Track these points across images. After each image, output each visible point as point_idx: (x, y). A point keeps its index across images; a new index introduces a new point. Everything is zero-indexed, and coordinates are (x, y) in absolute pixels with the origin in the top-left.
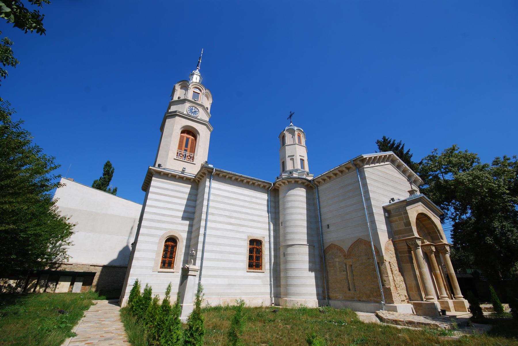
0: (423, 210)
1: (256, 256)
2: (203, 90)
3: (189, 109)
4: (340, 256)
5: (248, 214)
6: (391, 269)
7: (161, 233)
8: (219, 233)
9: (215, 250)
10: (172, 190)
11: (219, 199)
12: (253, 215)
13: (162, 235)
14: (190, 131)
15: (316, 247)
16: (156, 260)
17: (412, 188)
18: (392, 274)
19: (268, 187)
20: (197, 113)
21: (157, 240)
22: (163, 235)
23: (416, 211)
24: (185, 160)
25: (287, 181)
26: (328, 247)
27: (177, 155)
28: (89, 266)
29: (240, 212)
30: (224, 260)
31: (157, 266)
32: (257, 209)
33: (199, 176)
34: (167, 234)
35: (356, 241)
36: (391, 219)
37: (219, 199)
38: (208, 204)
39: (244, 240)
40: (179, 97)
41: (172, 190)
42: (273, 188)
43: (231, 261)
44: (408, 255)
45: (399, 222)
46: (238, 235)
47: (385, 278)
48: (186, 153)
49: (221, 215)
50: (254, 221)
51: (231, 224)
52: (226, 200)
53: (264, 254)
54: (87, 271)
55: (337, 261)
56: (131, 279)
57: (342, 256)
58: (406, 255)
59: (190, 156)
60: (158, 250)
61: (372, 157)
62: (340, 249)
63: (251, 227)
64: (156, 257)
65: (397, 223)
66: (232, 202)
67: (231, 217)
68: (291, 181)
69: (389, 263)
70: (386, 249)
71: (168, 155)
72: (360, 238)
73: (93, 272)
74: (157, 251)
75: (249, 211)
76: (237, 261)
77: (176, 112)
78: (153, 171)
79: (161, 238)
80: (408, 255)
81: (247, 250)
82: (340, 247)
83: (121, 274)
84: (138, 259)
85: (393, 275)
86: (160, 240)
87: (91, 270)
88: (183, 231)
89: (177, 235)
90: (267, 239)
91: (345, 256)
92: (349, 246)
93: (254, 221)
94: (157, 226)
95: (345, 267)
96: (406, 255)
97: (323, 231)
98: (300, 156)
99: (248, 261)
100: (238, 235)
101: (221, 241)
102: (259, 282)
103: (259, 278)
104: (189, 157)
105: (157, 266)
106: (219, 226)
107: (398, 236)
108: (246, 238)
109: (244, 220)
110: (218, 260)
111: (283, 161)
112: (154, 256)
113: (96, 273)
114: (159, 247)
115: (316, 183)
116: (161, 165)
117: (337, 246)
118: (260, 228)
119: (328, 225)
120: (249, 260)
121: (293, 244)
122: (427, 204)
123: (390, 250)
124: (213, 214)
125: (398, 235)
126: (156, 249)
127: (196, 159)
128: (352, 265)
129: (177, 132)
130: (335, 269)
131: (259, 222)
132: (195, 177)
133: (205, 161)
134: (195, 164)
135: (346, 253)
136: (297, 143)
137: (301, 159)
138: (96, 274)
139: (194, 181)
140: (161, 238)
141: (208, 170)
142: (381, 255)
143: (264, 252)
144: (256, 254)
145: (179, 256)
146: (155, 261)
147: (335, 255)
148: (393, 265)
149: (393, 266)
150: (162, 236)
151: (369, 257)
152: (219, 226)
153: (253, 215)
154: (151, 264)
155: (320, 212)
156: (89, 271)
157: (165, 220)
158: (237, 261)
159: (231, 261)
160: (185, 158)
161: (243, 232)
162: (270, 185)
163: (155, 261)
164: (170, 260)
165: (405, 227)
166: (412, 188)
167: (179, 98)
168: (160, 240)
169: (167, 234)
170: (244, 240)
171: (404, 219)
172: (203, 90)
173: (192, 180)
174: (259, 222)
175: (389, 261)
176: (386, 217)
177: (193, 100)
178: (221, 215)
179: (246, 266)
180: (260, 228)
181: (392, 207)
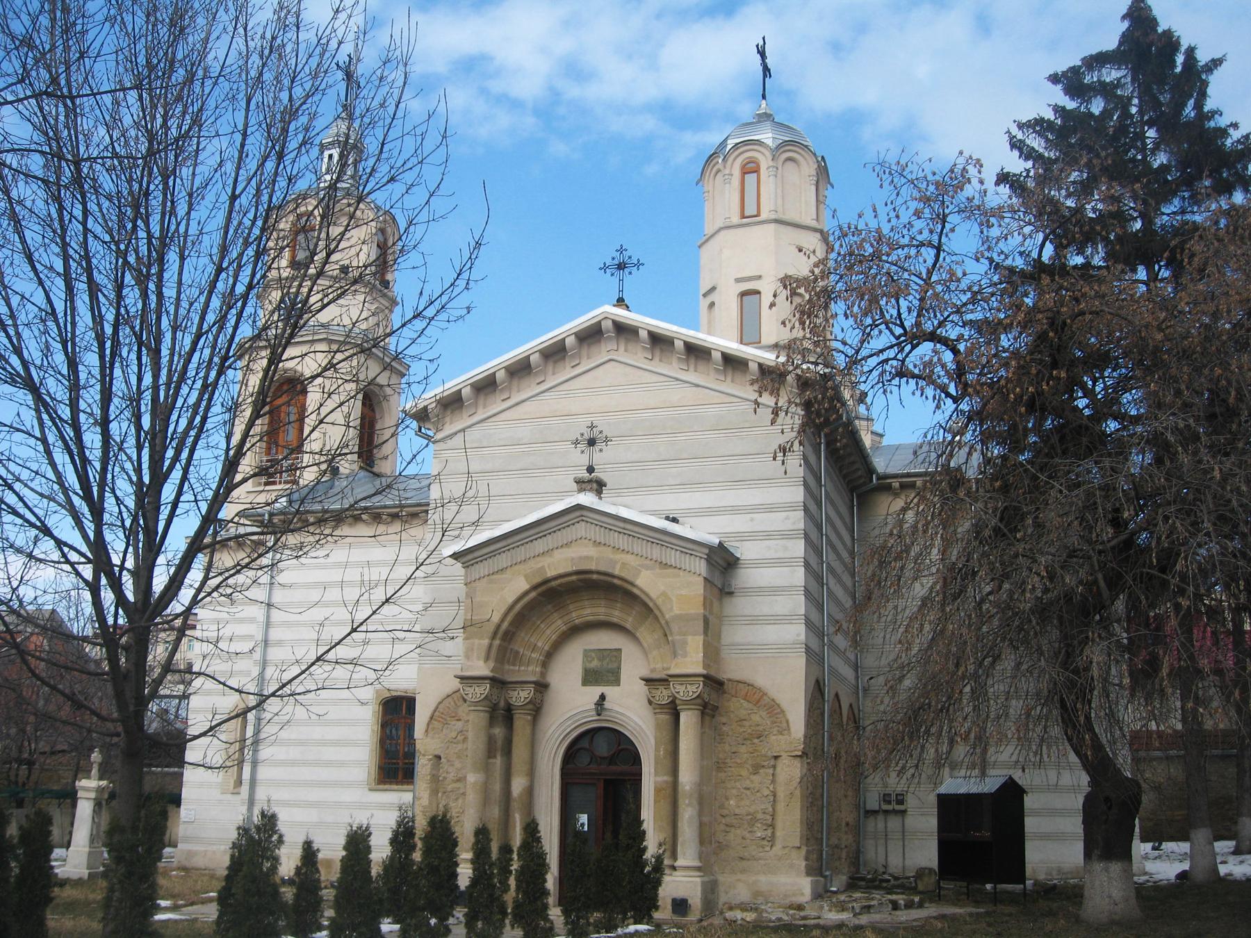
0: (588, 558)
17: (591, 469)
23: (526, 577)
24: (280, 483)
30: (305, 763)
43: (329, 764)
61: (460, 390)
81: (373, 731)
98: (738, 280)
110: (293, 763)
122: (621, 525)
123: (459, 720)
124: (280, 643)
148: (453, 765)
149: (450, 769)
158: (342, 764)
159: (329, 764)
166: (591, 469)
175: (436, 753)
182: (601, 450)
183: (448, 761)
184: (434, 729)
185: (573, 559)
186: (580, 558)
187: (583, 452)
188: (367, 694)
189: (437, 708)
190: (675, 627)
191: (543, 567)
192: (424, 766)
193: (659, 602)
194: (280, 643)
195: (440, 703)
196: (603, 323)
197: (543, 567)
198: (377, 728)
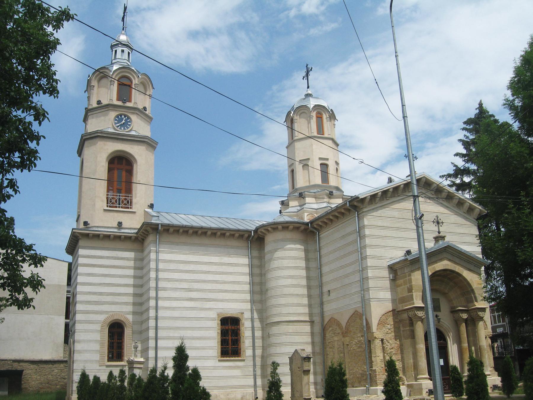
0: (448, 265)
1: (231, 339)
2: (134, 79)
3: (116, 120)
4: (339, 333)
5: (216, 282)
6: (383, 348)
7: (102, 318)
8: (176, 314)
9: (172, 336)
10: (108, 258)
11: (172, 266)
12: (224, 282)
13: (103, 320)
14: (122, 157)
15: (315, 322)
16: (101, 352)
17: (439, 232)
18: (384, 353)
19: (246, 235)
20: (129, 123)
21: (98, 327)
22: (105, 321)
24: (119, 207)
25: (271, 227)
26: (328, 322)
27: (107, 204)
28: (11, 362)
29: (204, 281)
31: (104, 359)
32: (231, 273)
33: (142, 234)
34: (109, 318)
35: (353, 314)
36: (397, 282)
37: (172, 266)
38: (157, 276)
39: (213, 319)
40: (98, 102)
41: (108, 258)
42: (256, 237)
44: (409, 328)
45: (404, 286)
46: (203, 314)
47: (373, 359)
48: (120, 196)
49: (176, 289)
50: (226, 291)
51: (191, 299)
52: (182, 267)
53: (243, 337)
54: (10, 369)
55: (336, 340)
56: (76, 375)
57: (340, 334)
58: (407, 328)
59: (126, 199)
60: (101, 339)
61: (378, 193)
62: (339, 324)
63: (222, 301)
64: (101, 348)
65: (402, 287)
66: (192, 267)
67: (190, 290)
68: (278, 228)
69: (382, 340)
70: (381, 323)
71: (94, 204)
72: (356, 311)
73: (18, 369)
74: (101, 341)
75: (218, 277)
76: (203, 348)
77: (97, 132)
78: (78, 235)
79: (103, 324)
80: (409, 328)
81: (218, 333)
82: (339, 322)
83: (57, 371)
84: (80, 352)
85: (386, 354)
86: (102, 327)
87: (16, 367)
88: (128, 313)
89: (122, 319)
90: (247, 315)
91: (343, 333)
92: (347, 321)
93: (226, 291)
94: (95, 310)
95: (342, 347)
96: (407, 328)
97: (324, 300)
98: (320, 159)
99: (220, 346)
100: (203, 314)
101: (179, 324)
102: (237, 372)
103: (238, 367)
104: (125, 202)
105: (104, 359)
106: (175, 304)
107: (402, 304)
108: (215, 316)
109: (210, 291)
111: (292, 168)
112: (97, 347)
113: (23, 371)
114: (102, 336)
115: (315, 226)
116: (88, 222)
117: (336, 320)
118: (237, 301)
119: (329, 291)
120: (222, 345)
121: (279, 320)
122: (458, 254)
123: (388, 324)
124: (164, 289)
125: (401, 304)
126: (100, 339)
127: (136, 203)
128: (348, 345)
129: (103, 166)
130: (334, 350)
131: (234, 292)
132: (137, 233)
133: (149, 204)
134: (135, 212)
135: (344, 329)
136: (315, 134)
137: (321, 164)
138: (24, 372)
139: (136, 239)
140: (103, 324)
141: (151, 228)
142: (372, 332)
143: (244, 333)
144: (231, 337)
145: (129, 346)
146: (101, 354)
147: (335, 332)
148: (389, 343)
149: (388, 344)
150: (104, 322)
151: (362, 334)
152: (175, 304)
153: (224, 282)
154: (97, 357)
155: (321, 272)
156: (13, 369)
157: (105, 301)
158: (203, 348)
160: (119, 204)
161: (210, 309)
162: (249, 233)
163: (101, 354)
164: (119, 351)
165: (408, 293)
166: (439, 232)
167: (99, 102)
168: (102, 327)
169: (109, 318)
170: (213, 319)
171: (408, 284)
172: (134, 79)
173: (133, 238)
174: (234, 292)
175: (382, 338)
176: (391, 279)
177: (120, 103)
178: (176, 289)
179: (218, 353)
180: (237, 301)
181: (397, 267)
182: (441, 226)
183: (387, 341)
184: (379, 328)
185: (443, 265)
186: (445, 264)
187: (436, 226)
188: (213, 315)
189: (380, 320)
190: (476, 291)
191: (435, 267)
192: (378, 343)
193: (470, 282)
194: (164, 289)
195: (381, 318)
196: (423, 179)
197: (435, 267)
198: (220, 331)
